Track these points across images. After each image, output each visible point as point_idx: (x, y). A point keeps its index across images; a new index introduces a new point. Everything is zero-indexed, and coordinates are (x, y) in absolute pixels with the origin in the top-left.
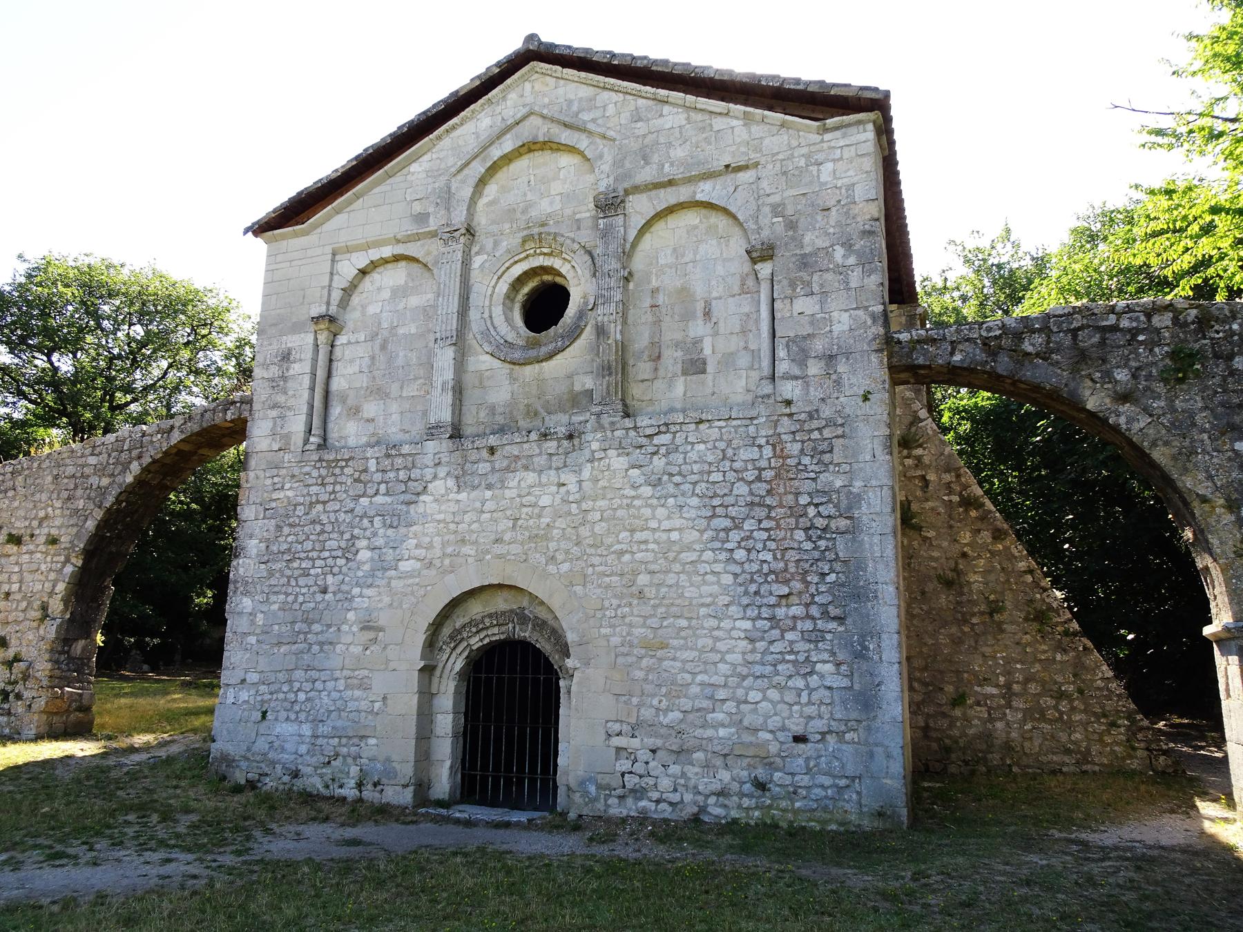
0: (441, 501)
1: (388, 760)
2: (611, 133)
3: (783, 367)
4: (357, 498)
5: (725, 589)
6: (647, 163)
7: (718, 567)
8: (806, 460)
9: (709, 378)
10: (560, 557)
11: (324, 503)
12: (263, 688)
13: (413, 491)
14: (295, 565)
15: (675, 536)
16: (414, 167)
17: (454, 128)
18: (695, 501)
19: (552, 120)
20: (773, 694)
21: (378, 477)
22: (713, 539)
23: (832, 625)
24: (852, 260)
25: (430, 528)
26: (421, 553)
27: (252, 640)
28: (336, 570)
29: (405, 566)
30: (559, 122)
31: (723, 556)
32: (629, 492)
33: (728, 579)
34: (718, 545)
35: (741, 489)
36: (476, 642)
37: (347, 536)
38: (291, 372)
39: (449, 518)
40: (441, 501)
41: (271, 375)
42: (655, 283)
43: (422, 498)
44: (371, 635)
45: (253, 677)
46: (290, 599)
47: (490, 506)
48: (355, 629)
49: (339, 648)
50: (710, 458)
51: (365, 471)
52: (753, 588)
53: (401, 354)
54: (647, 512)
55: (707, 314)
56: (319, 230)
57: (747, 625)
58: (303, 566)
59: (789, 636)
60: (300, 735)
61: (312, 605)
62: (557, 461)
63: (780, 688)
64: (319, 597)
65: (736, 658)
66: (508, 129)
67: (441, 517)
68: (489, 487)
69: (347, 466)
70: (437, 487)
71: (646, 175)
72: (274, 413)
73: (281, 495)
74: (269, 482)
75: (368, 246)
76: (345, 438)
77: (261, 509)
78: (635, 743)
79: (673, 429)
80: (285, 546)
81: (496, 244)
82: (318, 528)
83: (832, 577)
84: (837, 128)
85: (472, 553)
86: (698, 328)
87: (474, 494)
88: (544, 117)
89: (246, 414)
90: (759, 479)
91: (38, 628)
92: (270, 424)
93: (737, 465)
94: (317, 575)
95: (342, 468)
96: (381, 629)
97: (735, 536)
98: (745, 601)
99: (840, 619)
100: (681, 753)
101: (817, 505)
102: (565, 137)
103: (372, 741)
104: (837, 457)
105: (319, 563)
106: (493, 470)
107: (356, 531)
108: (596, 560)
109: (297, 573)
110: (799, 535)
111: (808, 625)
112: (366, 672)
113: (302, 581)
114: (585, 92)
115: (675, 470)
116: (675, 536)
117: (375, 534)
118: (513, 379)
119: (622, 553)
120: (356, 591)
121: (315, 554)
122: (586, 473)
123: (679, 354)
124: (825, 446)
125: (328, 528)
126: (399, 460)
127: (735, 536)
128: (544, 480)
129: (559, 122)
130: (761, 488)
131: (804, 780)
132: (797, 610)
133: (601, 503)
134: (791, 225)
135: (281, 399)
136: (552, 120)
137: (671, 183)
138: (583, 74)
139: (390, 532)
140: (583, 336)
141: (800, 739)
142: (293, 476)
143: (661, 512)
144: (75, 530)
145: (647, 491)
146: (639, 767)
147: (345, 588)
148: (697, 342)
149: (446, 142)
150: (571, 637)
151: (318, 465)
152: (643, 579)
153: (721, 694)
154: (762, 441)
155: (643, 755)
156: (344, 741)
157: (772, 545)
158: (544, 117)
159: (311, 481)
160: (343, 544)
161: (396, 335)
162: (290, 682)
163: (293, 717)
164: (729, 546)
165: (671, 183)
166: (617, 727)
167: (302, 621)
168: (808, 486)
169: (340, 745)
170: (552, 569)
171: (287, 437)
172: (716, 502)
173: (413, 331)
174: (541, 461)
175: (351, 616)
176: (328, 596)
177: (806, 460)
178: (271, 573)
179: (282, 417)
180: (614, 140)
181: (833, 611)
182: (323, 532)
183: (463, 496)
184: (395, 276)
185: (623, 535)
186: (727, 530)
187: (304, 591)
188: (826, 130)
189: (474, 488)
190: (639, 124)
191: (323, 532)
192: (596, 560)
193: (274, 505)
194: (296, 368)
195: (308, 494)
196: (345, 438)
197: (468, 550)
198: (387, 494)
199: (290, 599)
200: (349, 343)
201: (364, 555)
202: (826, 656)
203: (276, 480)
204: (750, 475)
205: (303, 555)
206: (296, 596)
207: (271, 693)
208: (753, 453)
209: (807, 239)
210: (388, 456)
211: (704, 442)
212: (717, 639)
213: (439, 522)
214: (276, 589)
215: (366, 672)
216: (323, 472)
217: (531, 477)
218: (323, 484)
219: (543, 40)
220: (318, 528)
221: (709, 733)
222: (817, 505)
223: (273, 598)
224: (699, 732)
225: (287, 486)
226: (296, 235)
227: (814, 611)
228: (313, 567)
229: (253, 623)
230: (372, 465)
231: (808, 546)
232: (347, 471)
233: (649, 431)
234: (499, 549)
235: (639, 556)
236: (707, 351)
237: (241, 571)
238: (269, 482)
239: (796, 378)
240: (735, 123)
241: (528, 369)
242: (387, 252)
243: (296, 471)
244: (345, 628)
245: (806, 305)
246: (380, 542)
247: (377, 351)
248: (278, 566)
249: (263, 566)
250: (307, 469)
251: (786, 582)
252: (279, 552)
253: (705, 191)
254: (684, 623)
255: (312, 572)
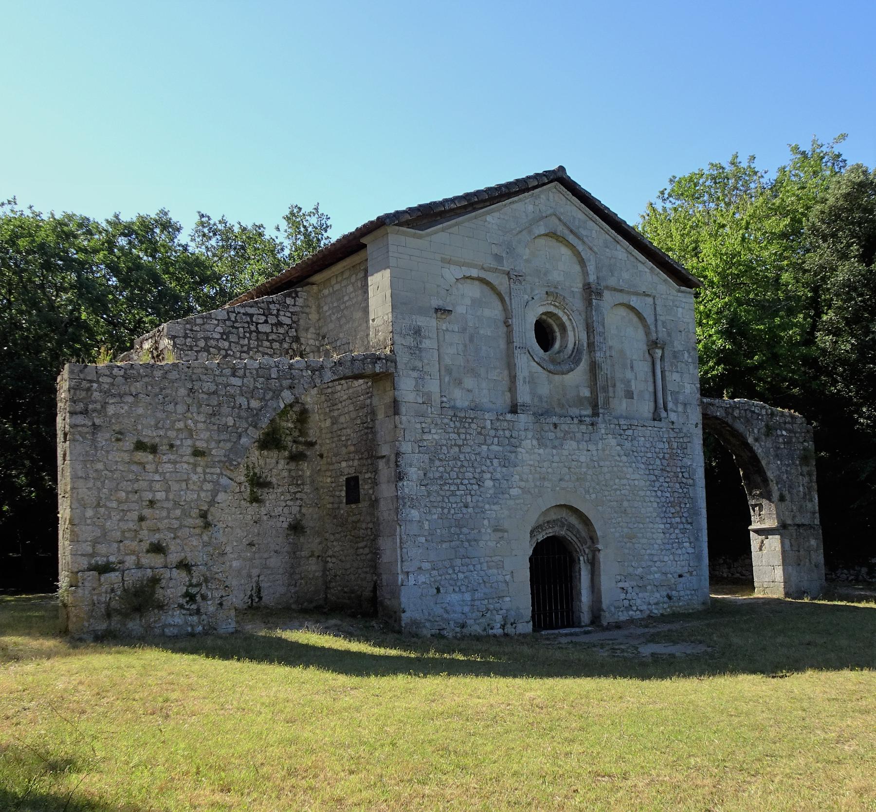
0: (529, 452)
1: (518, 608)
2: (595, 249)
3: (670, 405)
4: (480, 445)
5: (654, 509)
6: (613, 275)
7: (652, 499)
8: (679, 451)
9: (635, 401)
10: (591, 491)
11: (459, 446)
12: (435, 573)
13: (513, 444)
14: (447, 488)
15: (636, 482)
16: (489, 218)
17: (513, 202)
18: (643, 466)
19: (565, 224)
20: (671, 557)
21: (492, 433)
22: (650, 485)
23: (689, 526)
24: (690, 360)
25: (526, 469)
26: (523, 484)
27: (423, 540)
28: (473, 492)
29: (514, 492)
30: (568, 228)
31: (654, 494)
32: (617, 458)
33: (655, 505)
34: (651, 488)
35: (658, 462)
36: (540, 538)
37: (478, 470)
38: (423, 346)
39: (536, 464)
40: (529, 452)
41: (408, 344)
42: (610, 343)
43: (519, 449)
44: (500, 534)
45: (426, 566)
46: (446, 511)
47: (556, 459)
48: (489, 531)
49: (482, 544)
50: (648, 446)
51: (484, 428)
52: (664, 509)
53: (484, 348)
54: (625, 469)
55: (632, 367)
56: (429, 238)
57: (662, 526)
58: (452, 488)
59: (677, 531)
60: (463, 601)
61: (461, 515)
62: (586, 437)
63: (673, 554)
64: (464, 510)
65: (659, 542)
66: (542, 218)
67: (531, 463)
68: (554, 447)
69: (472, 422)
70: (527, 443)
71: (612, 282)
72: (415, 374)
73: (430, 437)
74: (418, 426)
75: (464, 264)
76: (454, 400)
77: (416, 446)
78: (625, 585)
79: (634, 427)
80: (437, 475)
81: (532, 290)
82: (459, 463)
83: (688, 506)
84: (682, 292)
85: (549, 486)
86: (629, 375)
87: (547, 451)
88: (560, 220)
89: (392, 370)
90: (664, 458)
91: (200, 535)
92: (414, 383)
93: (657, 450)
94: (462, 496)
95: (470, 423)
96: (506, 531)
97: (657, 484)
98: (662, 515)
99: (691, 523)
100: (642, 588)
101: (682, 473)
102: (571, 238)
103: (508, 599)
104: (689, 451)
105: (462, 487)
106: (556, 438)
107: (484, 468)
108: (606, 493)
109: (448, 493)
110: (678, 485)
111: (681, 526)
112: (499, 558)
113: (452, 499)
114: (580, 215)
115: (635, 449)
116: (636, 482)
117: (495, 470)
118: (550, 382)
119: (616, 490)
120: (487, 506)
121: (459, 481)
122: (600, 446)
123: (623, 386)
124: (684, 446)
125: (466, 464)
126: (506, 424)
127: (657, 484)
128: (581, 446)
129: (568, 228)
130: (665, 462)
131: (682, 593)
132: (678, 520)
133: (608, 463)
134: (669, 334)
135: (419, 364)
136: (565, 224)
137: (621, 291)
138: (583, 205)
139: (504, 469)
140: (581, 364)
141: (680, 576)
142: (436, 424)
143: (630, 470)
144: (229, 445)
145: (624, 458)
146: (629, 596)
147: (480, 504)
148: (629, 381)
149: (507, 210)
150: (599, 533)
151: (454, 419)
152: (625, 504)
153: (655, 559)
154: (665, 440)
155: (630, 590)
156: (491, 601)
157: (669, 490)
158: (560, 220)
159: (450, 430)
160: (477, 476)
161: (478, 333)
162: (453, 567)
163: (457, 589)
164: (656, 489)
165: (621, 291)
166: (619, 578)
167: (456, 526)
168: (679, 464)
169: (489, 603)
170: (587, 496)
171: (428, 395)
172: (651, 467)
173: (489, 334)
174: (579, 435)
175: (486, 522)
176: (470, 510)
177: (679, 451)
178: (429, 494)
179: (423, 379)
180: (596, 253)
181: (690, 520)
182: (462, 466)
183: (541, 451)
184: (474, 291)
185: (617, 481)
186: (654, 481)
187: (454, 506)
188: (679, 291)
189: (546, 446)
190: (607, 250)
191: (462, 466)
192: (606, 493)
193: (425, 444)
194: (426, 344)
195: (449, 439)
196: (454, 400)
197: (546, 484)
198: (498, 445)
199: (446, 511)
200: (447, 330)
201: (489, 483)
202: (687, 540)
203: (424, 425)
204: (661, 456)
205: (450, 481)
206: (449, 510)
207: (441, 576)
208: (661, 445)
209: (676, 343)
210: (498, 419)
211: (644, 437)
212: (653, 533)
213: (531, 465)
214: (435, 504)
215: (499, 558)
216: (458, 424)
217: (574, 444)
218: (459, 434)
219: (568, 174)
220: (459, 463)
221: (652, 577)
222: (682, 473)
223: (434, 511)
224: (648, 577)
225: (433, 431)
226: (414, 236)
227: (684, 520)
228: (458, 490)
229: (421, 528)
230: (489, 422)
231: (680, 491)
232: (474, 426)
233: (625, 427)
234: (563, 484)
235: (623, 492)
236: (633, 387)
237: (406, 490)
238: (418, 426)
239: (675, 412)
240: (647, 270)
241: (556, 377)
242: (474, 273)
243: (439, 422)
244: (483, 530)
245: (676, 376)
246: (498, 476)
247: (467, 342)
248: (435, 488)
249: (423, 488)
250: (446, 421)
251: (674, 507)
252: (434, 478)
253: (634, 301)
254: (641, 526)
255: (458, 493)
